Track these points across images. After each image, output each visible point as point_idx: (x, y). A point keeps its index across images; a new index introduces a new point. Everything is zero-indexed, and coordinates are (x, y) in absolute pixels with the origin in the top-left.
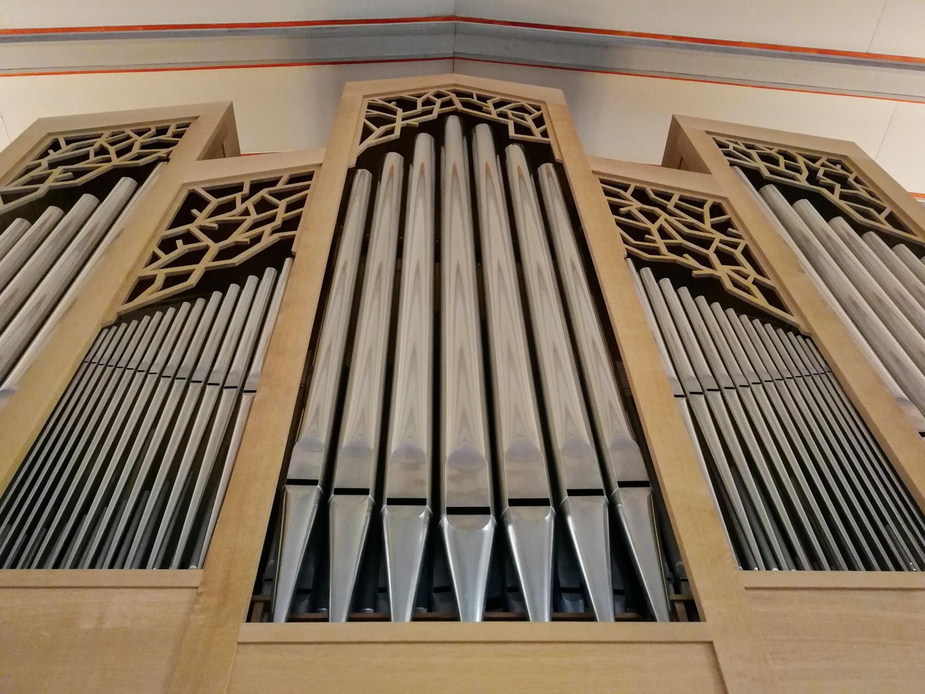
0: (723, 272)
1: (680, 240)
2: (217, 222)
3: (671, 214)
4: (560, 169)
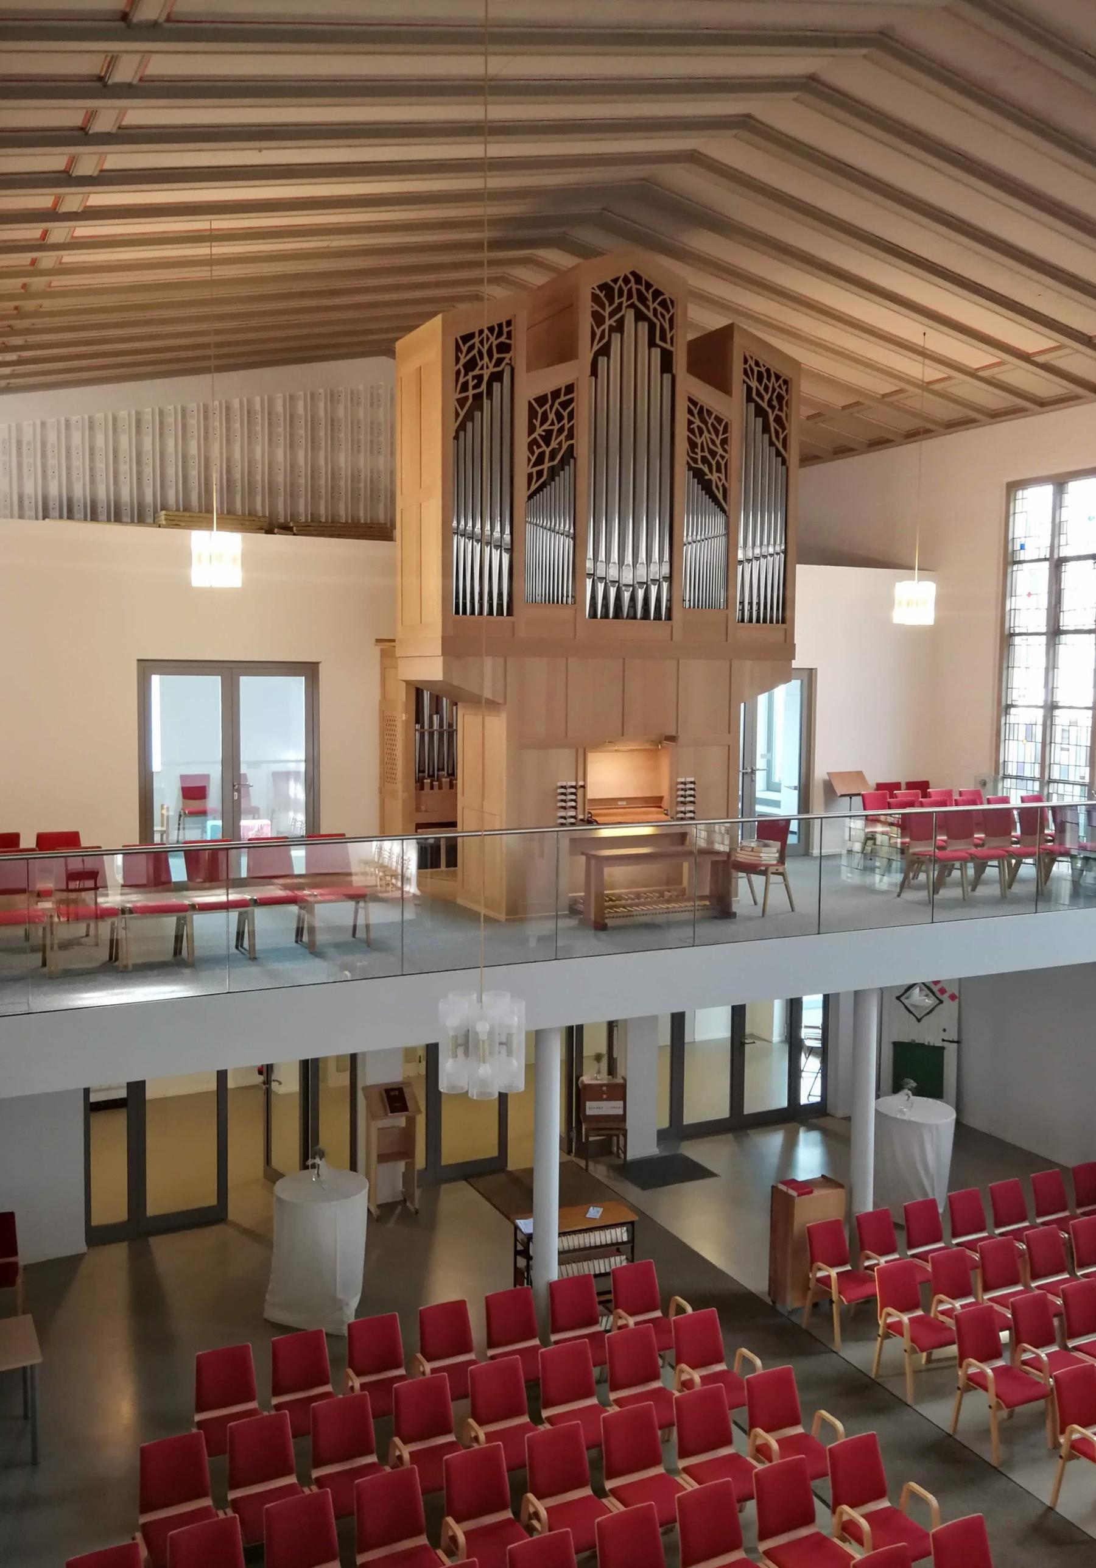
0: (714, 477)
1: (706, 454)
3: (709, 432)
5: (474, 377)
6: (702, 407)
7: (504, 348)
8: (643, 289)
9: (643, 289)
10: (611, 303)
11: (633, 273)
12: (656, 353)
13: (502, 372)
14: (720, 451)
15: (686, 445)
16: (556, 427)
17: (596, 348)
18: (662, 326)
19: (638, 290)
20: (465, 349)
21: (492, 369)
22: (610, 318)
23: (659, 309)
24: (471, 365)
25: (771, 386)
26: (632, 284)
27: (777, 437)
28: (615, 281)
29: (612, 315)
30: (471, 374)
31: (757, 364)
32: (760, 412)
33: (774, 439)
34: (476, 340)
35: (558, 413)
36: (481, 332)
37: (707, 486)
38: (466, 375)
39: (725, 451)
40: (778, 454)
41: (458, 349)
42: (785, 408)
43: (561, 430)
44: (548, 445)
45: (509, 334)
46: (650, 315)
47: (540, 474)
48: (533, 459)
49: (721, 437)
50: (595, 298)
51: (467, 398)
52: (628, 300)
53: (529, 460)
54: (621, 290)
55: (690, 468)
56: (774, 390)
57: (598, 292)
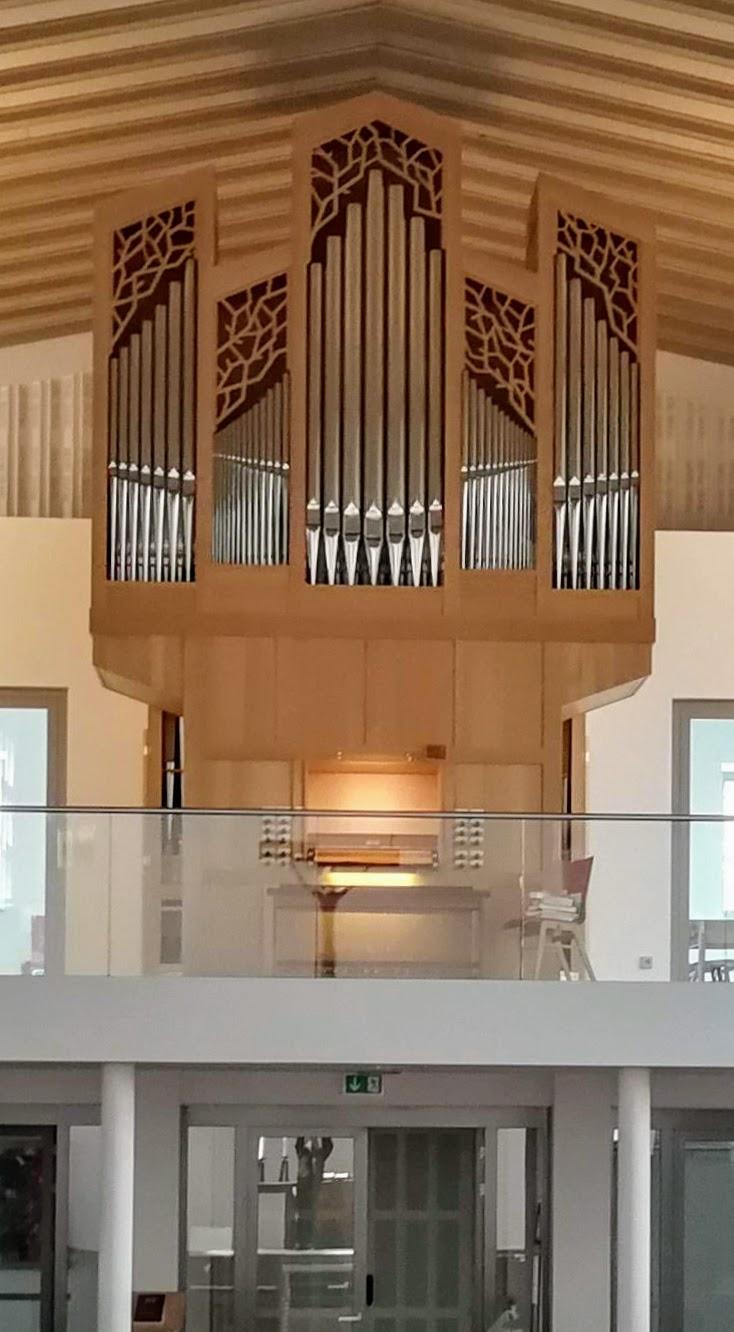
0: (512, 384)
1: (498, 354)
2: (241, 339)
3: (501, 323)
4: (444, 253)
5: (140, 278)
6: (489, 291)
7: (184, 238)
8: (391, 142)
9: (391, 142)
10: (342, 164)
11: (377, 124)
12: (418, 226)
13: (183, 266)
14: (520, 348)
15: (464, 344)
16: (260, 333)
17: (319, 225)
18: (422, 189)
19: (385, 146)
20: (127, 244)
21: (164, 266)
22: (340, 185)
23: (418, 166)
24: (134, 265)
25: (605, 252)
26: (376, 139)
27: (619, 323)
28: (349, 137)
29: (342, 181)
30: (136, 274)
31: (581, 224)
32: (589, 290)
33: (615, 328)
34: (144, 232)
35: (262, 314)
36: (150, 220)
37: (500, 399)
38: (128, 276)
39: (531, 348)
40: (623, 347)
41: (118, 245)
42: (631, 281)
43: (263, 342)
44: (247, 356)
45: (191, 221)
46: (405, 174)
47: (235, 395)
48: (225, 376)
49: (521, 329)
50: (317, 162)
51: (128, 306)
52: (368, 159)
53: (219, 378)
54: (357, 149)
55: (472, 375)
56: (611, 258)
57: (322, 153)
